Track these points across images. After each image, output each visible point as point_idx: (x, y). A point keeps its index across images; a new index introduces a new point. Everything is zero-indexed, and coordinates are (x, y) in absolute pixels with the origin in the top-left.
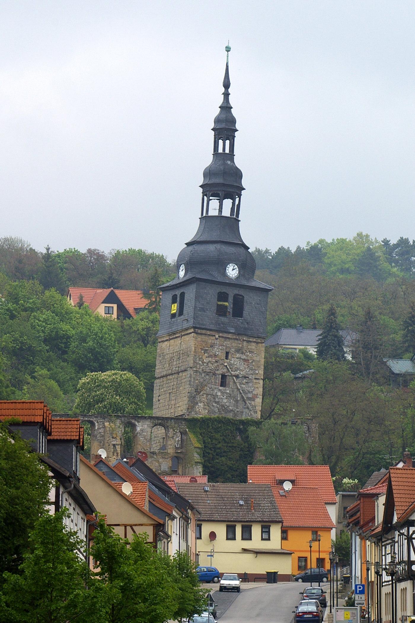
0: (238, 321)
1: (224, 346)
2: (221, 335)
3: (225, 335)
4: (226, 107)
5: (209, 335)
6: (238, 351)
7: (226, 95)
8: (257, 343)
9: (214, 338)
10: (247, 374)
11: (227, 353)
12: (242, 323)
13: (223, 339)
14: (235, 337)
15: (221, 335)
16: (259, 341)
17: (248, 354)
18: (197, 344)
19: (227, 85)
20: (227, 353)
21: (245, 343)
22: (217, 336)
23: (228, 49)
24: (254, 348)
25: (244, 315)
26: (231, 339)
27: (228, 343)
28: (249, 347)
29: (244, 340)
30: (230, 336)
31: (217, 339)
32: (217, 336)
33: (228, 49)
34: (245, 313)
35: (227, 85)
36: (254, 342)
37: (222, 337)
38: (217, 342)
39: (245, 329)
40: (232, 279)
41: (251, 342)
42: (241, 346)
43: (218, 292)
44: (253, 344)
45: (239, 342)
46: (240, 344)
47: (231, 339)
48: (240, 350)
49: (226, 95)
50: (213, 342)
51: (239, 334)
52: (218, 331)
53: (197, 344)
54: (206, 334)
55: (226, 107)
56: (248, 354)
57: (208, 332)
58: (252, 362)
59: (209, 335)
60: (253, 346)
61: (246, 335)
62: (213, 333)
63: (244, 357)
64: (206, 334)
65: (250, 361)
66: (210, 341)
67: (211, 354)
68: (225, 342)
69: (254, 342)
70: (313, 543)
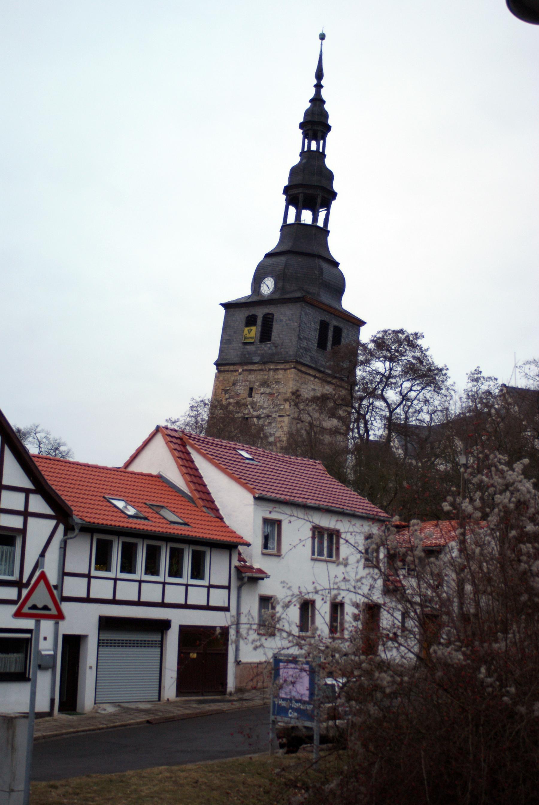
0: (266, 347)
1: (247, 381)
2: (245, 368)
3: (251, 367)
4: (317, 101)
5: (232, 371)
6: (264, 383)
7: (319, 87)
8: (285, 370)
9: (237, 373)
10: (271, 412)
11: (251, 389)
12: (270, 348)
13: (246, 373)
14: (260, 367)
15: (245, 368)
16: (288, 367)
17: (274, 386)
18: (218, 385)
19: (319, 75)
20: (251, 389)
21: (271, 373)
22: (240, 370)
23: (322, 37)
24: (280, 376)
25: (273, 337)
26: (255, 370)
27: (252, 377)
28: (276, 377)
29: (270, 370)
30: (255, 367)
31: (240, 374)
32: (240, 370)
33: (322, 37)
34: (275, 336)
35: (319, 75)
36: (282, 369)
37: (246, 370)
38: (240, 378)
39: (273, 355)
40: (264, 297)
41: (278, 369)
42: (266, 377)
43: (246, 316)
44: (281, 372)
45: (265, 373)
46: (265, 375)
47: (255, 370)
48: (265, 382)
49: (319, 87)
50: (236, 378)
51: (264, 363)
52: (240, 364)
53: (218, 385)
54: (228, 371)
55: (317, 101)
56: (274, 386)
57: (232, 368)
58: (278, 395)
59: (232, 371)
60: (280, 375)
61: (272, 362)
62: (236, 367)
63: (268, 390)
64: (228, 371)
65: (276, 395)
66: (233, 378)
67: (233, 393)
68: (250, 376)
69: (282, 369)
70: (76, 519)
